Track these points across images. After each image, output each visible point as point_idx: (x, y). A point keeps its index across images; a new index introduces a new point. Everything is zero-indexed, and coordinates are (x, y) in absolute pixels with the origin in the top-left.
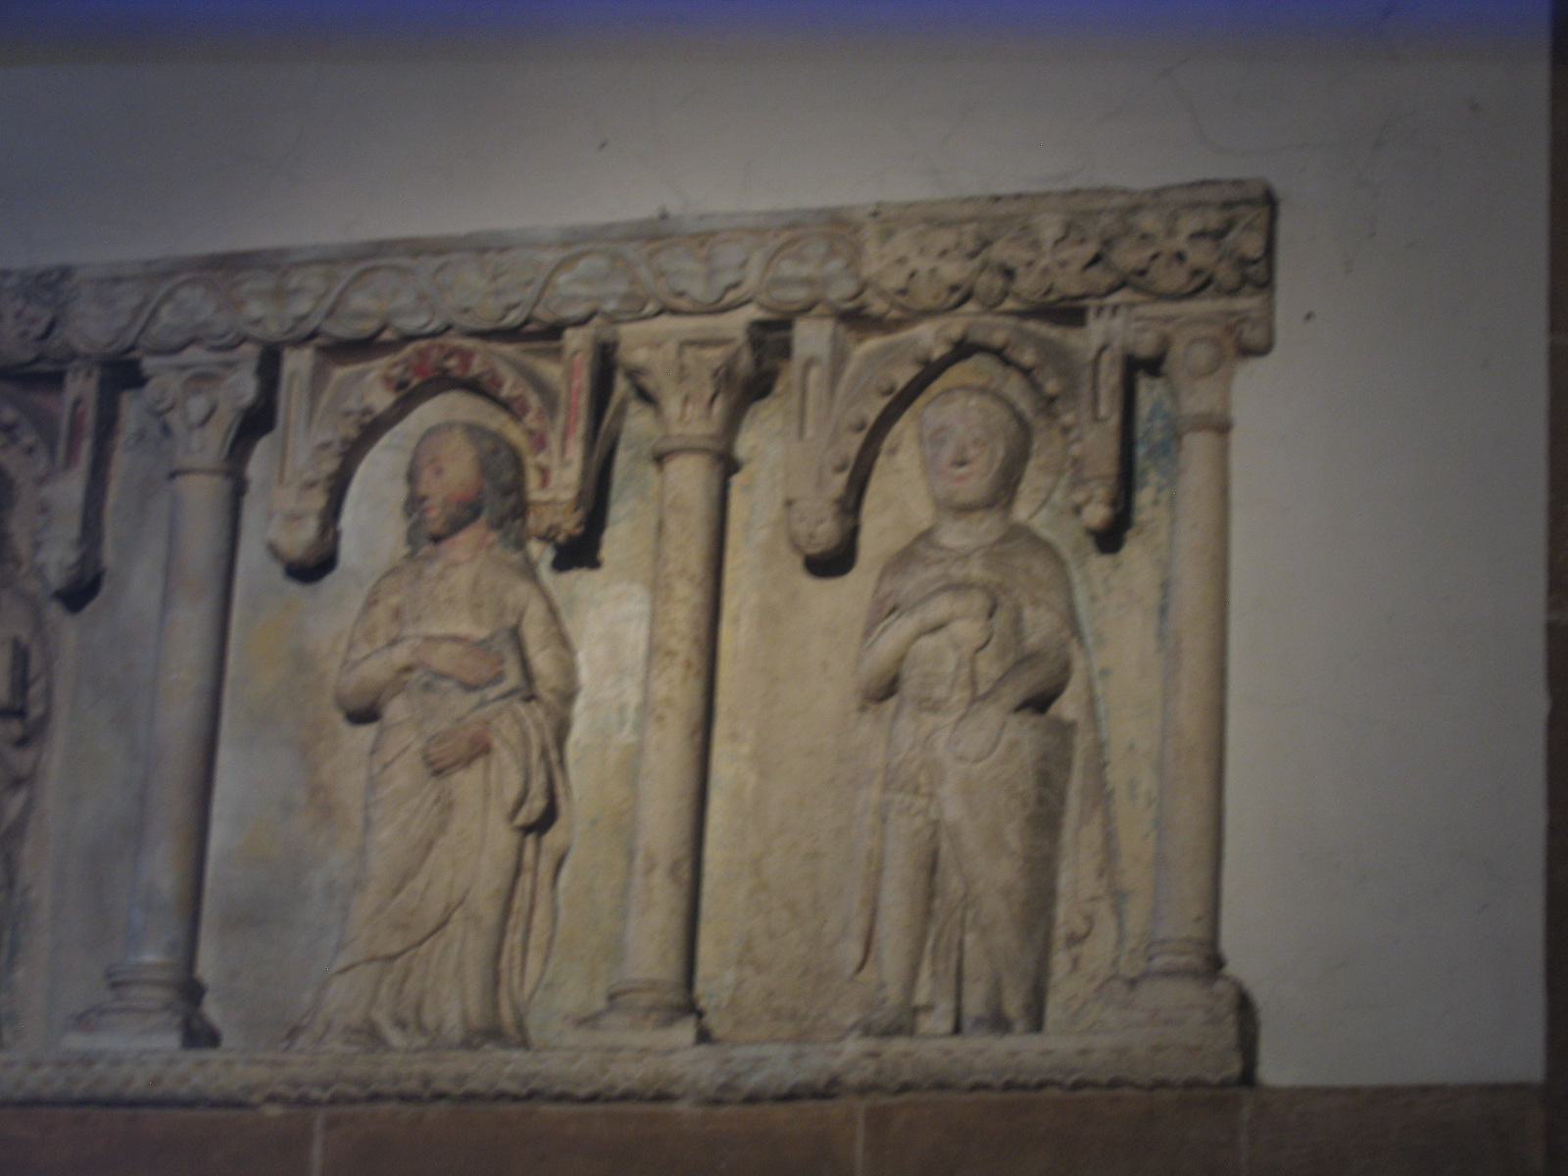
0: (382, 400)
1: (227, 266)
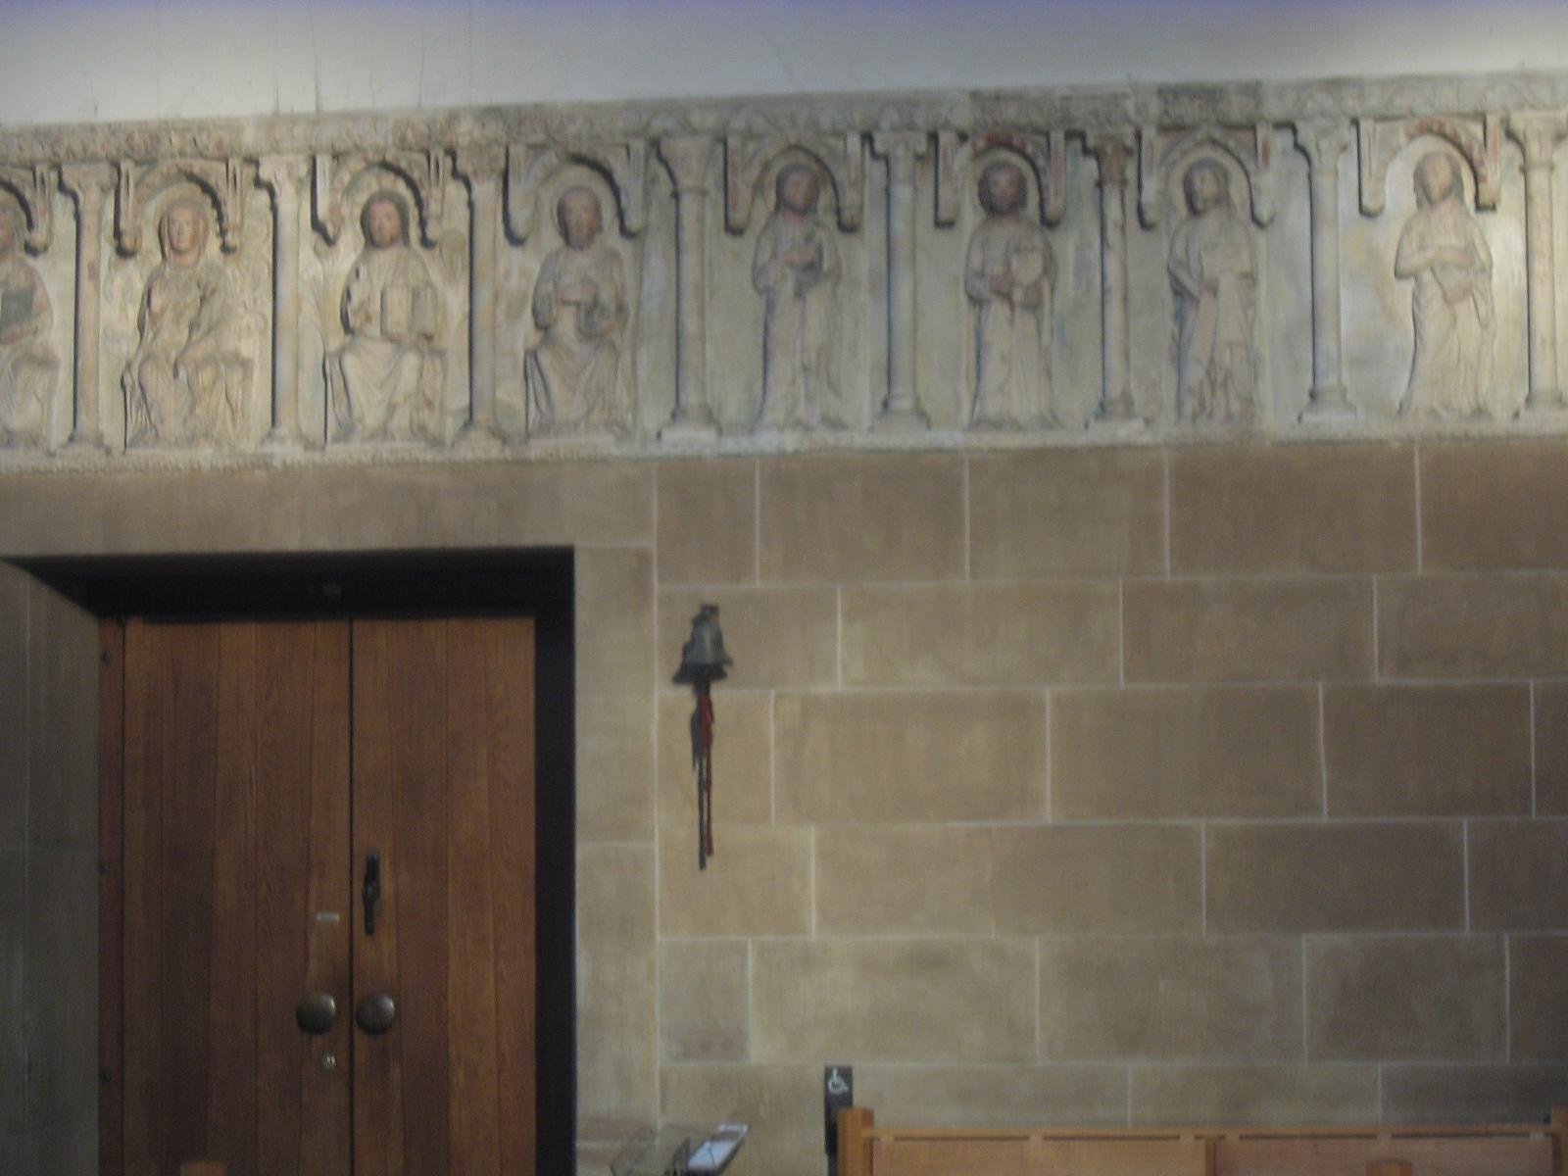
0: (1402, 139)
1: (1335, 85)
